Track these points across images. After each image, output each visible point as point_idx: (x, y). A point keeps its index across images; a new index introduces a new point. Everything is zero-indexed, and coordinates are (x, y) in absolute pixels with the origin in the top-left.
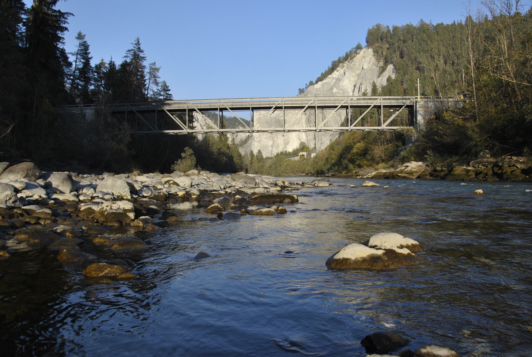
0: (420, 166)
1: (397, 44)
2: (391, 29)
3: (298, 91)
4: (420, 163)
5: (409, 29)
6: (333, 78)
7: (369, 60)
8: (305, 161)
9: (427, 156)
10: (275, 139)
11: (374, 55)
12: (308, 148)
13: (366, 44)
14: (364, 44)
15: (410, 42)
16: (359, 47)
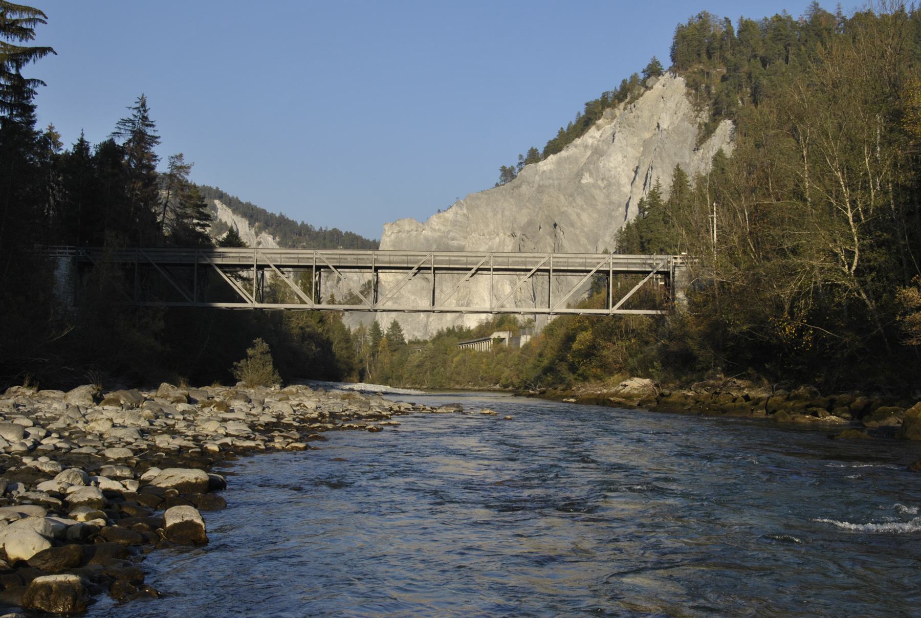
0: (646, 386)
3: (500, 173)
4: (647, 381)
6: (586, 147)
7: (673, 106)
8: (502, 354)
9: (654, 370)
11: (688, 94)
13: (671, 64)
14: (666, 62)
15: (780, 62)
16: (654, 71)
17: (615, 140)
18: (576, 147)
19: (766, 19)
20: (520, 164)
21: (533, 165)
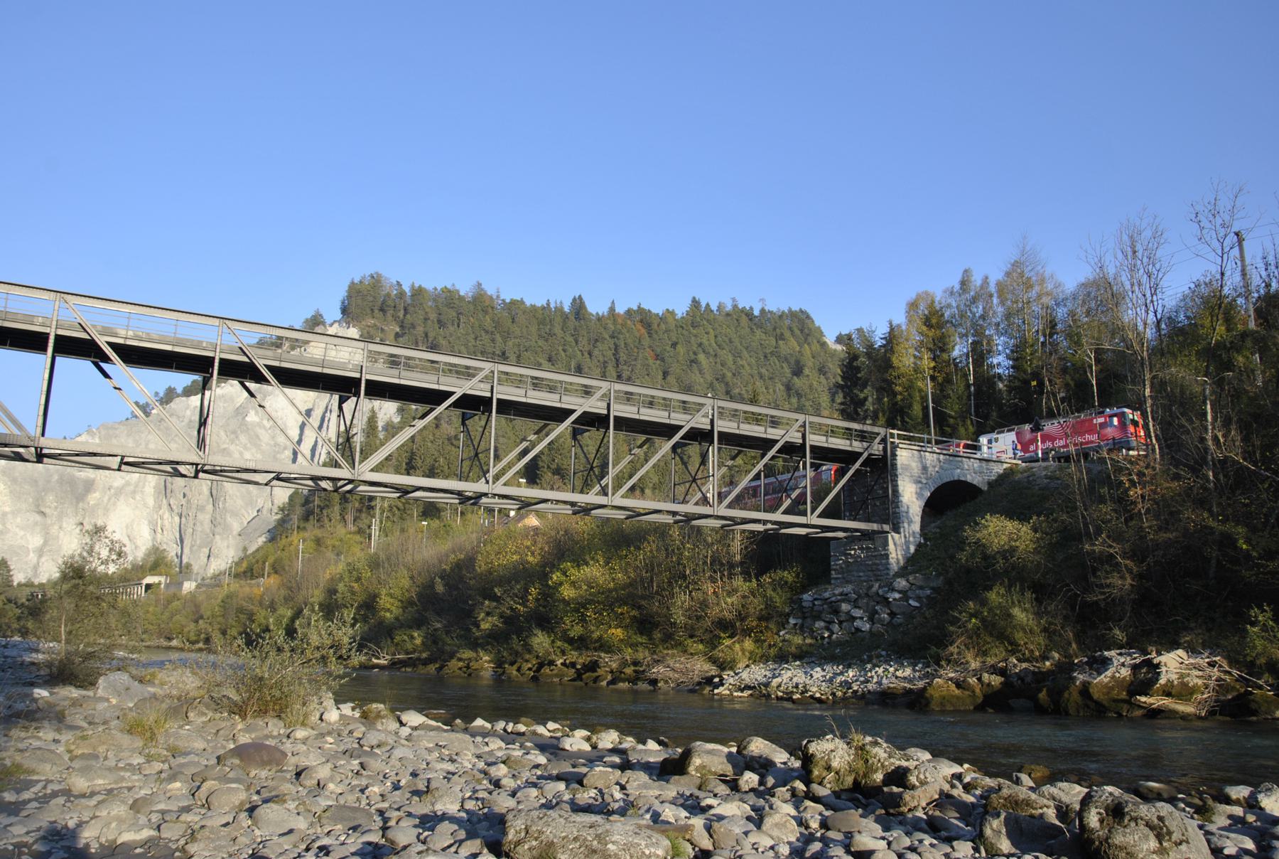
1: (420, 330)
2: (406, 288)
5: (449, 299)
10: (54, 530)
12: (169, 565)
13: (339, 316)
14: (332, 312)
19: (436, 289)
21: (184, 399)
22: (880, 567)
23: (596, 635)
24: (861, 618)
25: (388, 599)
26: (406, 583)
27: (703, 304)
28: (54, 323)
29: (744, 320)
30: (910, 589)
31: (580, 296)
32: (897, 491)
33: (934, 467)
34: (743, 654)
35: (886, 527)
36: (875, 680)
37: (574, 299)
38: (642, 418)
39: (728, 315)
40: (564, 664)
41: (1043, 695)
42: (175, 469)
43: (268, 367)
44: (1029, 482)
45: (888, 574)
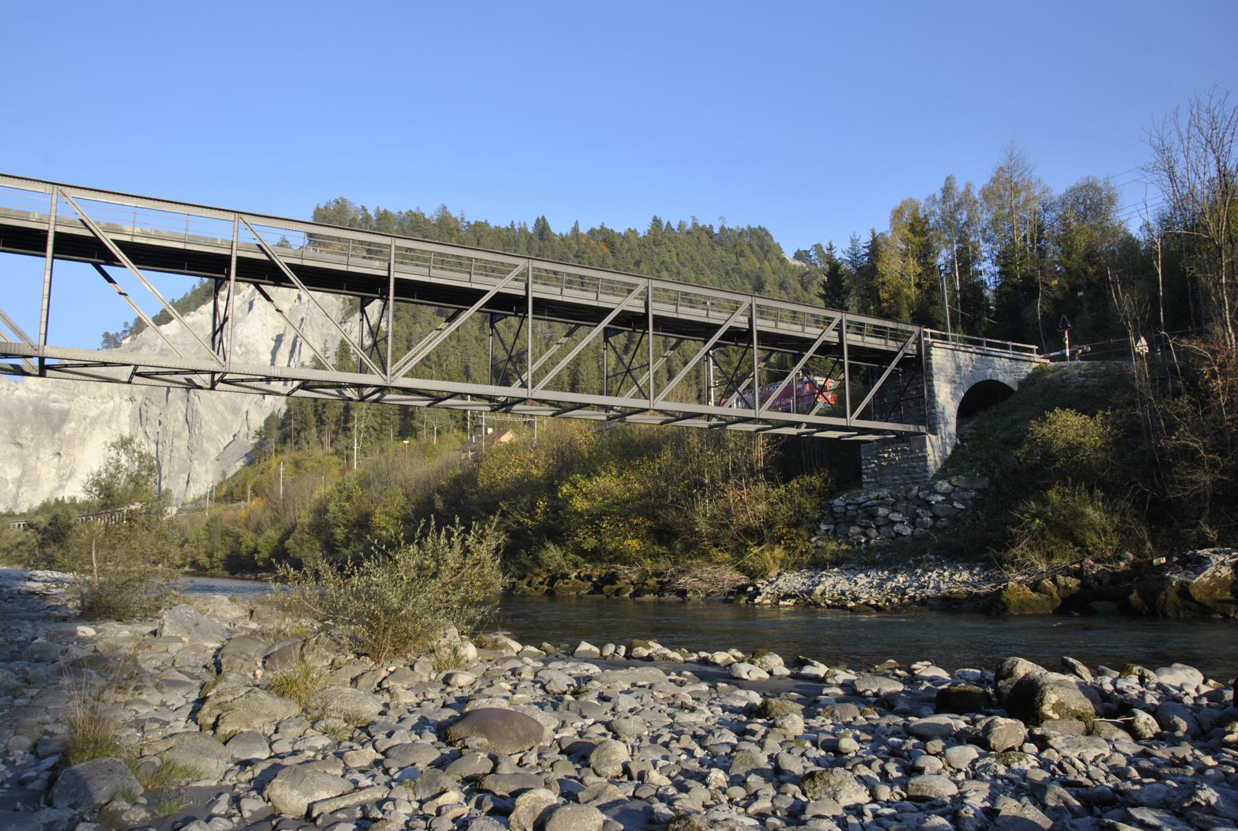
2: (372, 212)
3: (102, 339)
10: (32, 460)
17: (254, 308)
18: (202, 314)
19: (400, 213)
20: (125, 331)
22: (918, 470)
23: (611, 546)
24: (902, 522)
25: (383, 517)
26: (400, 500)
27: (664, 224)
28: (53, 219)
29: (705, 238)
30: (953, 491)
31: (543, 217)
32: (933, 392)
33: (967, 366)
34: (774, 562)
35: (923, 429)
36: (932, 585)
37: (538, 220)
38: (681, 317)
39: (688, 233)
40: (576, 577)
41: (1134, 596)
42: (190, 381)
43: (291, 266)
44: (1063, 380)
45: (926, 477)
